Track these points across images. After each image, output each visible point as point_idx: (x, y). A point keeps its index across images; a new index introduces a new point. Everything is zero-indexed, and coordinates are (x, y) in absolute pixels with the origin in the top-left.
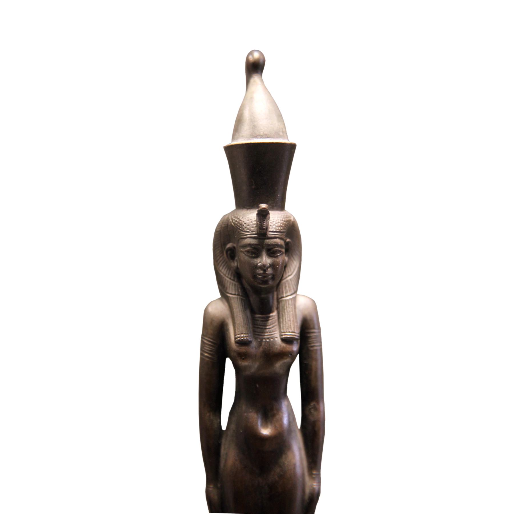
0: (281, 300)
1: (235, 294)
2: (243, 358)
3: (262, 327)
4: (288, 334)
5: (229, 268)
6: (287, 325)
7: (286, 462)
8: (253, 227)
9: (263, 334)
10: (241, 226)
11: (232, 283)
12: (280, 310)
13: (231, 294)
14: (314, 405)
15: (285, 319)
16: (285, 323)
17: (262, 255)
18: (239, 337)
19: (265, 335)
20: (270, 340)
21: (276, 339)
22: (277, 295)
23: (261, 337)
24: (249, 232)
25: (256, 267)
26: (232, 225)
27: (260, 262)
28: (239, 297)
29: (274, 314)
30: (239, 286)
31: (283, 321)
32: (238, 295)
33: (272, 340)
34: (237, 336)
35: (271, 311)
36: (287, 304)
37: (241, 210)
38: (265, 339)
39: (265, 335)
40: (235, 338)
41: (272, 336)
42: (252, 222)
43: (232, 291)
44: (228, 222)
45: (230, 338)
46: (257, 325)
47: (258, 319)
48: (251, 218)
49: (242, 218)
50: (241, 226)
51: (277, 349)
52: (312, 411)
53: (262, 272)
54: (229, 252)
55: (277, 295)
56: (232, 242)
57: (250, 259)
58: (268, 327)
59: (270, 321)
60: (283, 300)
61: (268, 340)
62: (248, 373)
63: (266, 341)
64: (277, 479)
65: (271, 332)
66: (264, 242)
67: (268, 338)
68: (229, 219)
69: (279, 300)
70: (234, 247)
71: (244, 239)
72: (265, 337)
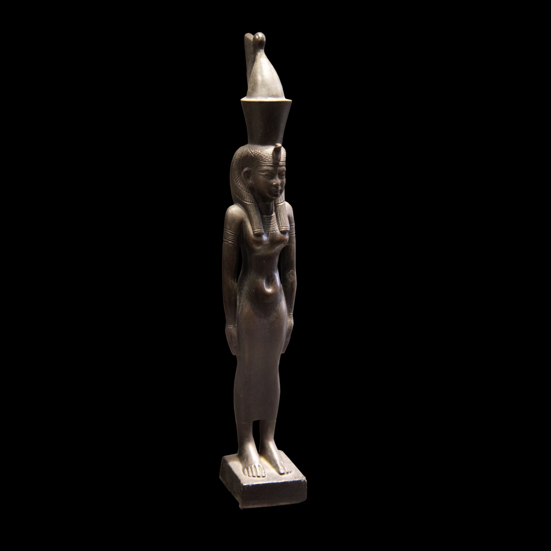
0: (278, 205)
1: (250, 202)
2: (259, 244)
3: (268, 224)
4: (283, 229)
5: (245, 184)
6: (284, 222)
7: (279, 309)
8: (270, 159)
9: (269, 228)
10: (260, 157)
11: (248, 195)
12: (277, 211)
13: (248, 202)
14: (292, 271)
15: (282, 218)
16: (282, 221)
17: (276, 178)
18: (257, 231)
19: (270, 229)
20: (273, 232)
21: (277, 231)
22: (275, 202)
23: (268, 230)
24: (267, 162)
25: (272, 185)
26: (252, 156)
27: (274, 182)
28: (253, 204)
29: (274, 214)
30: (252, 196)
31: (281, 219)
32: (253, 202)
33: (274, 232)
34: (255, 230)
35: (272, 213)
36: (282, 208)
37: (257, 145)
38: (270, 231)
39: (270, 229)
40: (254, 232)
41: (274, 229)
42: (269, 155)
43: (248, 200)
44: (248, 154)
45: (249, 232)
46: (265, 222)
47: (265, 218)
48: (268, 152)
49: (261, 152)
50: (260, 157)
51: (278, 237)
52: (291, 275)
53: (275, 189)
54: (246, 174)
55: (275, 202)
56: (248, 167)
57: (267, 180)
58: (271, 224)
59: (272, 220)
60: (279, 205)
61: (272, 232)
62: (259, 254)
63: (271, 233)
64: (275, 319)
65: (273, 227)
66: (277, 169)
67: (272, 231)
68: (249, 152)
69: (276, 206)
70: (250, 170)
71: (263, 167)
72: (270, 230)
